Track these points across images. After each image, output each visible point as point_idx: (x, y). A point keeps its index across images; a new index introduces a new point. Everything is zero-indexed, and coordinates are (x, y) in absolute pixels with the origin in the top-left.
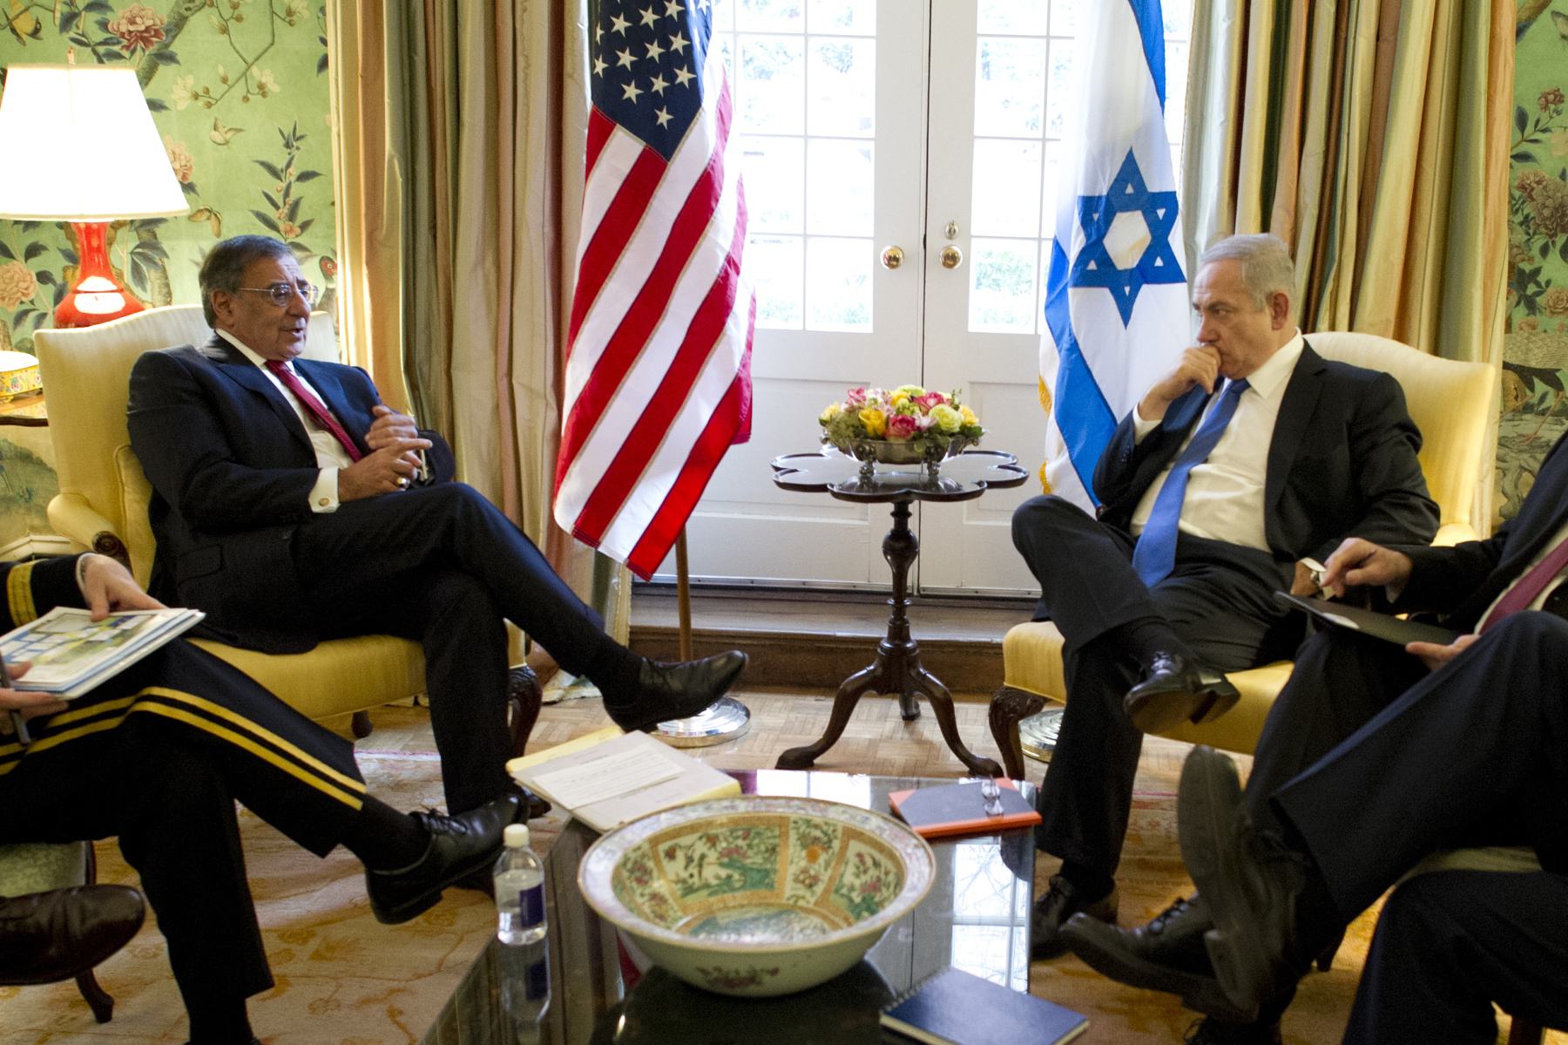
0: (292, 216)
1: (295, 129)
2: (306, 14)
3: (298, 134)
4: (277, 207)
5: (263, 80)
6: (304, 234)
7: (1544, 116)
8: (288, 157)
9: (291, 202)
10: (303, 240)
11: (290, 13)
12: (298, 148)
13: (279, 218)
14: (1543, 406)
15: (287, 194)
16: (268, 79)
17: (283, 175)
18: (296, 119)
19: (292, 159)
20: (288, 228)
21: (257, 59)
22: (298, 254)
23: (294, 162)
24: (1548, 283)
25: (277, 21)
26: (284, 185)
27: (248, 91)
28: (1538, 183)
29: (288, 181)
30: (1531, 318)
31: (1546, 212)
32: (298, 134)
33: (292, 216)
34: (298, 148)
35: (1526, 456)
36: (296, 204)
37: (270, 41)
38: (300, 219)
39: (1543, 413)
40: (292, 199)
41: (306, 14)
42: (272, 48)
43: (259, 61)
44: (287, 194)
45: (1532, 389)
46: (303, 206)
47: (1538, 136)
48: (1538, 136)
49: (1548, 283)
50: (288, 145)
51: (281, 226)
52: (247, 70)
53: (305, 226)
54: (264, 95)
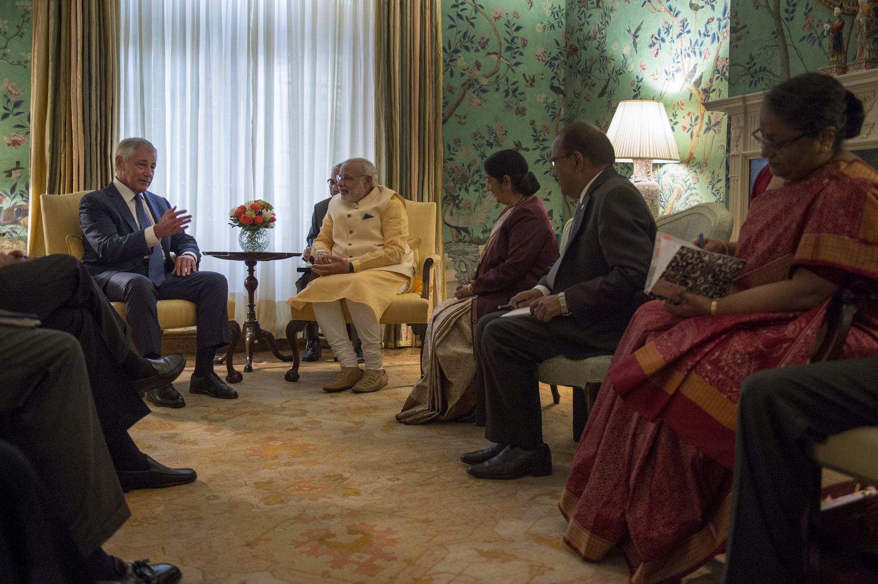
7: (456, 147)
14: (465, 240)
24: (462, 199)
28: (456, 167)
30: (458, 211)
31: (459, 177)
35: (461, 257)
39: (465, 242)
45: (461, 234)
47: (454, 153)
48: (454, 153)
49: (462, 199)
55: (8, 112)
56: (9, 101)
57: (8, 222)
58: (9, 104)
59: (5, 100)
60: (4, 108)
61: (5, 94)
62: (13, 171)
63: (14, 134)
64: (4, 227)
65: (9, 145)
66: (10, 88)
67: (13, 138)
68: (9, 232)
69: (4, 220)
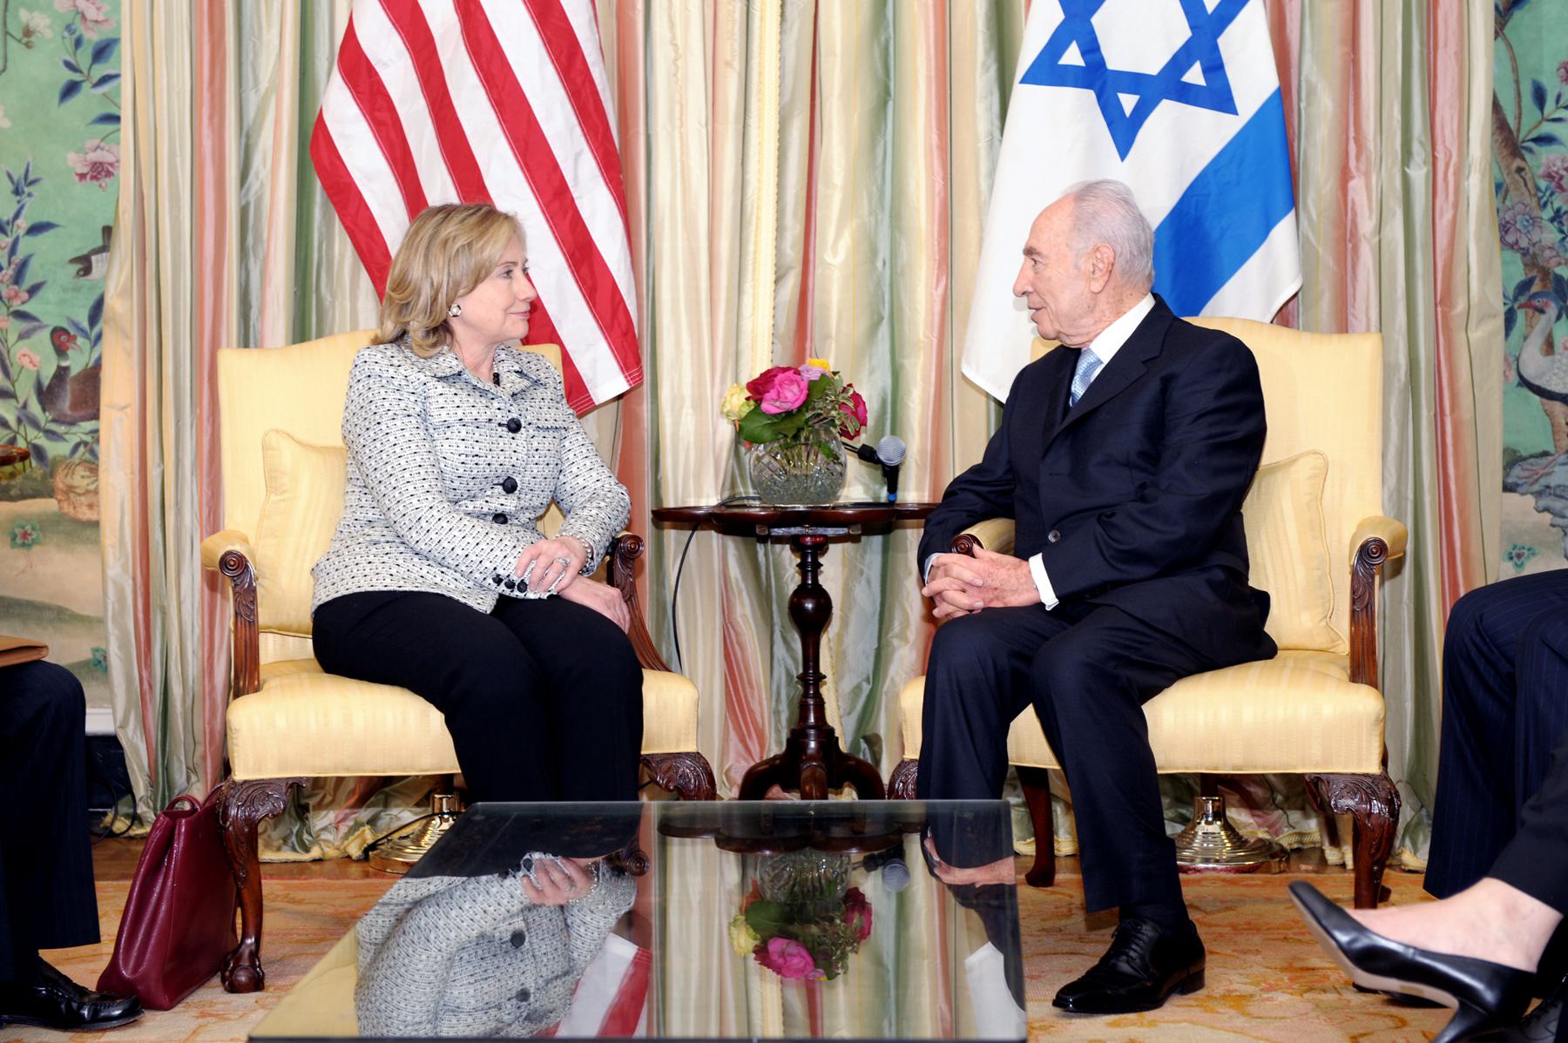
0: (18, 278)
1: (27, 171)
2: (48, 34)
3: (31, 177)
8: (17, 207)
9: (18, 261)
10: (30, 308)
11: (28, 32)
12: (30, 195)
15: (13, 251)
17: (8, 229)
18: (30, 160)
19: (22, 208)
20: (12, 293)
22: (23, 326)
23: (24, 212)
25: (12, 44)
26: (10, 240)
29: (14, 236)
32: (31, 177)
34: (30, 195)
36: (23, 265)
38: (28, 282)
41: (48, 34)
44: (13, 251)
46: (34, 266)
50: (17, 192)
53: (33, 291)
55: (76, 77)
56: (78, 43)
58: (80, 51)
59: (70, 43)
60: (68, 65)
61: (69, 21)
62: (94, 258)
63: (96, 142)
64: (74, 429)
65: (82, 176)
68: (86, 444)
69: (74, 406)
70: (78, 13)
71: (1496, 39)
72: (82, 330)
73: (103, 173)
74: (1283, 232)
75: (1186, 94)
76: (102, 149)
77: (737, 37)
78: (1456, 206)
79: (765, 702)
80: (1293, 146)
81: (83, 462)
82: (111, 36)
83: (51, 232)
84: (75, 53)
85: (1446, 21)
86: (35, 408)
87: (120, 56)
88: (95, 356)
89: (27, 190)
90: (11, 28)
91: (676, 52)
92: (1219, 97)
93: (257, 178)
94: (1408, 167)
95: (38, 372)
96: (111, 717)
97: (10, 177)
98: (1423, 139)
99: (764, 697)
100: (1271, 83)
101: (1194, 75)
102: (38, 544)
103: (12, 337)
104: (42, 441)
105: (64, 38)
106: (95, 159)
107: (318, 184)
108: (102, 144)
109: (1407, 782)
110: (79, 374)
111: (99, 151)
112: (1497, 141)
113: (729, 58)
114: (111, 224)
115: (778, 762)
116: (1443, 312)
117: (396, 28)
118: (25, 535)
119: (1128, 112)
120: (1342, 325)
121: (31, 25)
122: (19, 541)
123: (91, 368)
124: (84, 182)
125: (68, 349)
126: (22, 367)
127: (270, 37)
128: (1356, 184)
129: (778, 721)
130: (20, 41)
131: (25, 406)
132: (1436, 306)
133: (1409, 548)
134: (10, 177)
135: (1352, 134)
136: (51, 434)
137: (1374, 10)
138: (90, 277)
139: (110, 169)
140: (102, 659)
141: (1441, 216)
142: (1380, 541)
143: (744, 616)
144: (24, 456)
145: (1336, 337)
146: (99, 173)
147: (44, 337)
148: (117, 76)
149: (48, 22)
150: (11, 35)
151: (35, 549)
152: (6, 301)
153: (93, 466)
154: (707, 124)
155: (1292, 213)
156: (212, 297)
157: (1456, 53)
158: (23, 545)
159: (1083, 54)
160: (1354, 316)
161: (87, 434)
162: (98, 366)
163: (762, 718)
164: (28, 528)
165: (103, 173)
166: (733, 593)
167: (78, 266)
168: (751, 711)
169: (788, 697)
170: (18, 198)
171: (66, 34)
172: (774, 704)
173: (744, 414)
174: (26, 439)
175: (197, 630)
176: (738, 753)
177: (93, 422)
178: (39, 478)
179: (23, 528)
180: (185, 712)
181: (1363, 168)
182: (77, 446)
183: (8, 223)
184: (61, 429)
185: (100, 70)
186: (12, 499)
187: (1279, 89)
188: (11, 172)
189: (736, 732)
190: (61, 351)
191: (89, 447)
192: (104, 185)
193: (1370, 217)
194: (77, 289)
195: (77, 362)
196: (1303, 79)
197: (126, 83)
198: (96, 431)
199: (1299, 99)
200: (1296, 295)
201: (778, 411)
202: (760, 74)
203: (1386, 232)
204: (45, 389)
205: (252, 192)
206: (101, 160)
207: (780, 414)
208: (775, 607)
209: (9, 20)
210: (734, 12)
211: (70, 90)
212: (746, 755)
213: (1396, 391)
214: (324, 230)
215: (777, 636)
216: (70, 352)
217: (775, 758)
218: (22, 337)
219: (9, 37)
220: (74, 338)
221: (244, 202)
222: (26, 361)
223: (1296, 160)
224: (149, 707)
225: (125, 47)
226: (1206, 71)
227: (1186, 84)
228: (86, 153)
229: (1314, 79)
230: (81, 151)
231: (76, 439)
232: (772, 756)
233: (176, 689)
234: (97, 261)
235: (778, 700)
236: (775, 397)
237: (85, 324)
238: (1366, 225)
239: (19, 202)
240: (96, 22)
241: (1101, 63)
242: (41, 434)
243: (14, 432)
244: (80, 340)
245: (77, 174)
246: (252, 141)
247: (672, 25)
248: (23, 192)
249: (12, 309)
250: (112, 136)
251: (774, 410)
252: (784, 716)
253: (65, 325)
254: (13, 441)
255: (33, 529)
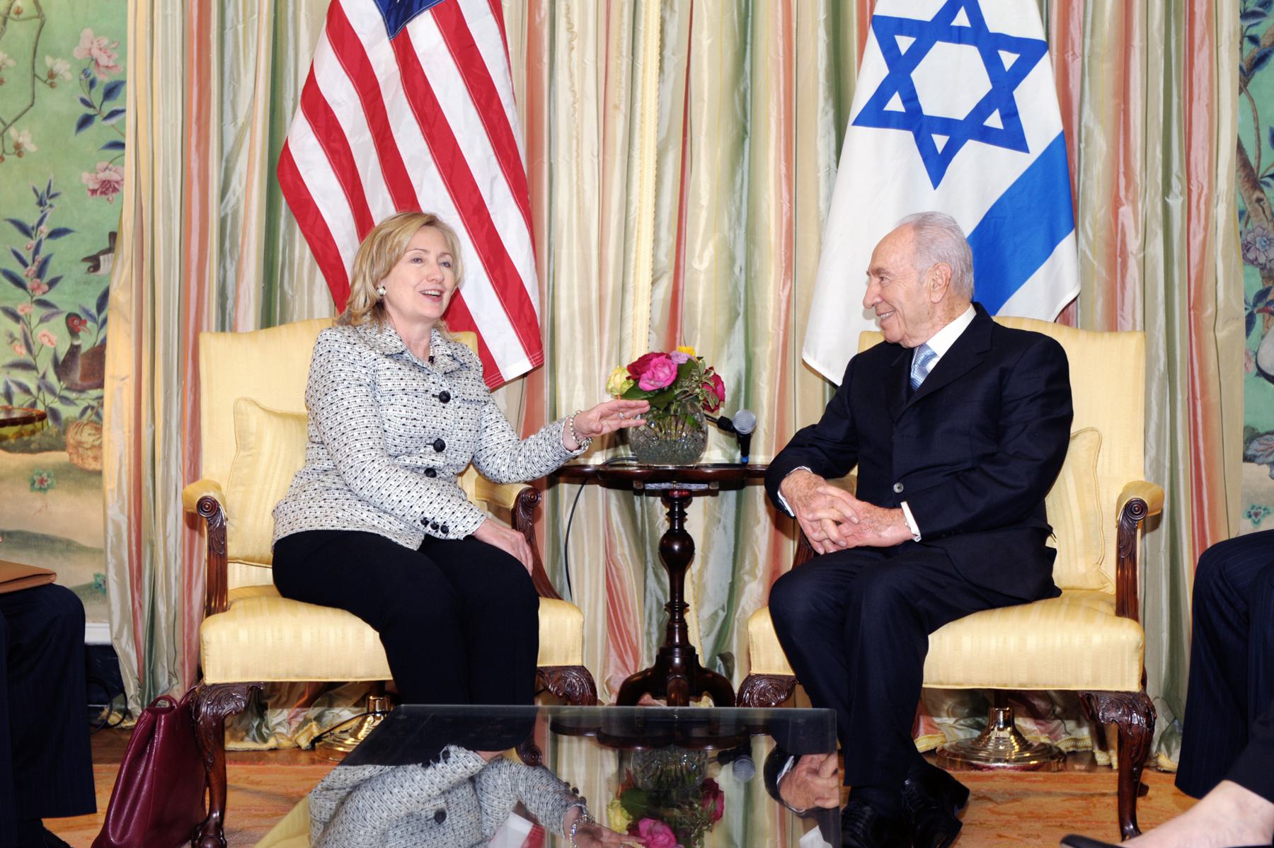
0: (40, 273)
1: (49, 187)
2: (68, 76)
3: (52, 192)
4: (25, 264)
5: (21, 140)
6: (52, 291)
8: (40, 216)
11: (52, 75)
12: (51, 206)
13: (27, 276)
15: (37, 251)
16: (26, 140)
20: (36, 285)
21: (15, 120)
22: (44, 311)
23: (46, 220)
25: (39, 84)
26: (34, 242)
27: (4, 151)
32: (52, 192)
33: (40, 273)
34: (51, 206)
36: (45, 262)
37: (29, 102)
38: (49, 276)
40: (40, 257)
41: (68, 76)
42: (32, 108)
43: (17, 123)
44: (37, 251)
50: (41, 203)
51: (29, 284)
52: (4, 131)
53: (52, 283)
54: (20, 154)
55: (90, 111)
56: (92, 84)
57: (90, 383)
58: (93, 91)
59: (86, 83)
60: (84, 102)
62: (102, 258)
63: (105, 164)
64: (83, 396)
65: (94, 192)
66: (96, 52)
67: (102, 176)
68: (93, 408)
69: (84, 377)
70: (92, 60)
71: (1240, 94)
72: (91, 316)
73: (111, 190)
74: (1066, 247)
75: (987, 136)
76: (110, 170)
77: (624, 85)
78: (1206, 229)
79: (639, 625)
80: (1073, 179)
81: (89, 422)
82: (118, 78)
83: (68, 236)
84: (89, 93)
85: (1199, 80)
86: (52, 378)
87: (125, 95)
88: (101, 337)
89: (49, 202)
90: (38, 71)
91: (575, 97)
92: (1013, 138)
93: (234, 194)
94: (1168, 197)
95: (55, 348)
96: (109, 630)
97: (35, 191)
98: (1180, 174)
99: (638, 620)
100: (1056, 127)
101: (994, 121)
102: (52, 488)
103: (35, 321)
104: (57, 405)
105: (81, 80)
106: (104, 179)
107: (284, 200)
108: (110, 166)
109: (1163, 699)
110: (88, 352)
111: (107, 172)
112: (1240, 176)
113: (617, 102)
114: (116, 230)
115: (649, 673)
116: (1194, 315)
117: (349, 76)
118: (42, 481)
119: (940, 149)
120: (1112, 325)
121: (55, 69)
122: (37, 485)
123: (98, 347)
124: (94, 196)
125: (79, 331)
126: (42, 345)
127: (247, 81)
128: (1125, 210)
129: (650, 641)
130: (45, 82)
131: (44, 377)
132: (1190, 310)
133: (1166, 507)
134: (35, 191)
135: (1122, 169)
136: (64, 400)
137: (1141, 70)
138: (98, 273)
139: (116, 186)
140: (102, 583)
141: (1195, 236)
142: (1142, 501)
143: (623, 555)
144: (42, 417)
145: (1107, 335)
146: (107, 189)
147: (59, 322)
148: (123, 111)
149: (68, 66)
150: (38, 77)
151: (50, 492)
152: (30, 292)
153: (98, 426)
154: (598, 156)
155: (1073, 233)
156: (196, 289)
157: (1207, 105)
158: (41, 489)
159: (904, 102)
160: (1122, 316)
161: (94, 400)
162: (103, 344)
163: (637, 638)
164: (45, 475)
165: (111, 190)
166: (615, 536)
167: (89, 264)
168: (628, 632)
169: (658, 622)
170: (42, 208)
171: (83, 77)
172: (646, 625)
173: (625, 391)
174: (44, 404)
175: (179, 561)
176: (616, 667)
177: (99, 390)
178: (54, 435)
179: (41, 475)
180: (168, 626)
181: (1131, 197)
182: (85, 410)
183: (33, 228)
184: (73, 395)
185: (109, 106)
186: (32, 452)
187: (1063, 132)
188: (36, 187)
189: (616, 650)
190: (74, 332)
191: (95, 410)
192: (111, 199)
193: (1136, 237)
194: (87, 283)
195: (86, 342)
196: (1082, 124)
197: (130, 116)
198: (101, 398)
199: (1080, 141)
200: (1075, 299)
201: (653, 388)
202: (642, 115)
203: (1149, 250)
204: (60, 362)
205: (231, 204)
206: (108, 178)
207: (654, 390)
208: (648, 548)
209: (36, 65)
210: (621, 65)
211: (85, 121)
212: (624, 669)
213: (1157, 379)
214: (287, 237)
215: (650, 571)
216: (81, 334)
217: (647, 670)
218: (42, 320)
219: (36, 79)
220: (85, 322)
221: (223, 214)
222: (45, 340)
223: (1076, 190)
224: (139, 621)
225: (129, 88)
226: (1004, 117)
227: (987, 128)
228: (97, 173)
229: (1091, 125)
230: (94, 171)
231: (85, 404)
232: (644, 669)
233: (162, 608)
234: (104, 260)
235: (650, 624)
236: (650, 377)
237: (94, 311)
238: (1134, 244)
239: (42, 212)
240: (107, 67)
241: (919, 110)
242: (56, 399)
243: (34, 397)
244: (90, 324)
245: (90, 190)
246: (231, 165)
247: (571, 76)
248: (46, 204)
249: (35, 298)
250: (119, 159)
251: (649, 388)
252: (655, 637)
253: (77, 311)
254: (34, 405)
255: (49, 476)
